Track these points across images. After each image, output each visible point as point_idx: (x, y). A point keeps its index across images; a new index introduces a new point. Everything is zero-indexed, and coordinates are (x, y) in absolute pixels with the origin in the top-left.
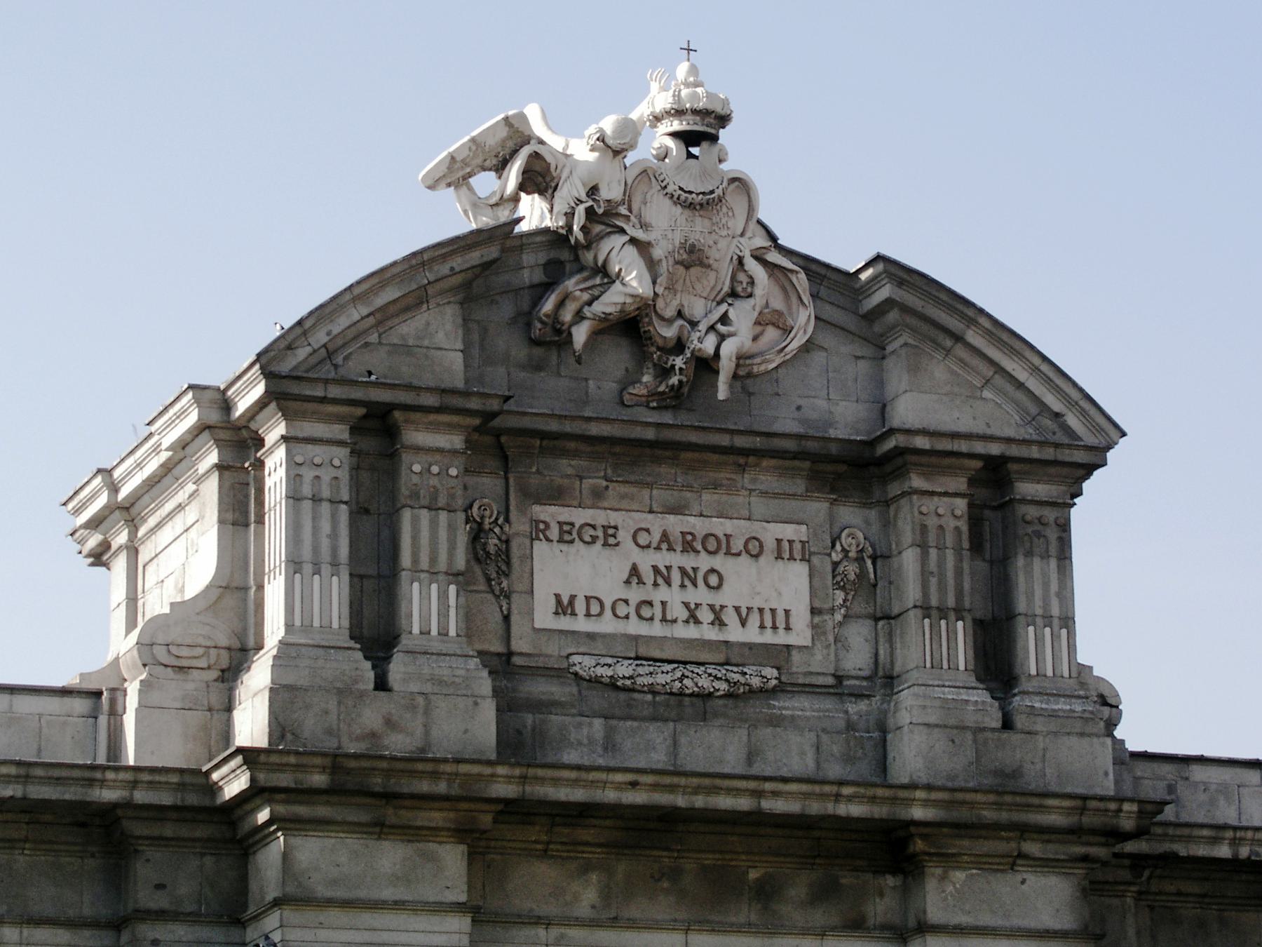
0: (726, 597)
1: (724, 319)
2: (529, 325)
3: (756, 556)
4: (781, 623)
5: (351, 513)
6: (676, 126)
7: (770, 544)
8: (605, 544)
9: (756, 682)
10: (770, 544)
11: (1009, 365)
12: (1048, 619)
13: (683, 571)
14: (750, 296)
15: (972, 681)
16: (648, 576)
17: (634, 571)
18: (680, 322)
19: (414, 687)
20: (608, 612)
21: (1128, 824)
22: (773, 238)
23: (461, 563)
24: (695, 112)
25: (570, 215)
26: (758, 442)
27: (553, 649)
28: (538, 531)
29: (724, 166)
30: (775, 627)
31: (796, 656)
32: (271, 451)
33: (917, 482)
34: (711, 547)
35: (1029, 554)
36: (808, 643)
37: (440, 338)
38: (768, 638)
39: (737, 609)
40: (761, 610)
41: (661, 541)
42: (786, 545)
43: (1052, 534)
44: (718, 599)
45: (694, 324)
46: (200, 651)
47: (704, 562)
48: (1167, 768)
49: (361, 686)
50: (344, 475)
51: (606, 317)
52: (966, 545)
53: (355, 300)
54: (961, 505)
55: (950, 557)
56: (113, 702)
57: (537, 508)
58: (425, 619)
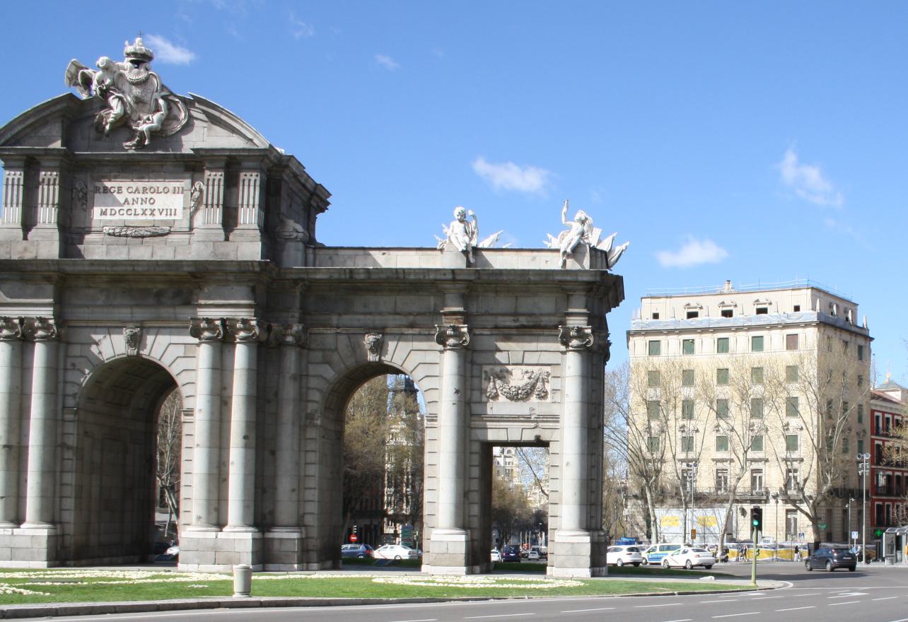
1: (148, 119)
3: (166, 193)
10: (171, 189)
15: (220, 226)
16: (131, 202)
19: (35, 239)
23: (56, 201)
30: (171, 215)
36: (181, 218)
38: (169, 218)
39: (159, 210)
40: (167, 210)
42: (177, 189)
47: (149, 196)
48: (331, 252)
51: (112, 123)
55: (216, 188)
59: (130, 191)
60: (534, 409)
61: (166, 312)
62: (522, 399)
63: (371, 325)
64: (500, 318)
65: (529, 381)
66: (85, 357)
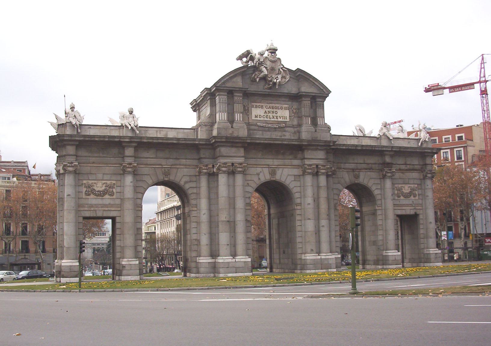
0: (279, 114)
1: (277, 77)
2: (251, 79)
4: (285, 118)
5: (227, 104)
6: (270, 51)
7: (284, 108)
8: (262, 108)
9: (282, 126)
10: (284, 108)
11: (316, 83)
12: (321, 117)
13: (272, 111)
14: (281, 74)
15: (311, 125)
16: (267, 112)
17: (266, 111)
18: (271, 78)
20: (262, 116)
21: (332, 144)
22: (284, 66)
24: (273, 49)
25: (256, 64)
26: (282, 94)
27: (255, 122)
28: (253, 106)
29: (276, 57)
31: (287, 122)
32: (217, 96)
33: (303, 99)
34: (276, 108)
35: (319, 108)
37: (239, 81)
38: (284, 120)
39: (279, 116)
41: (269, 107)
42: (286, 108)
43: (322, 106)
44: (277, 115)
45: (273, 78)
46: (208, 123)
47: (275, 110)
49: (229, 128)
50: (226, 99)
52: (310, 107)
53: (228, 76)
54: (309, 102)
55: (308, 108)
56: (197, 130)
57: (252, 103)
58: (238, 119)
59: (266, 107)
60: (413, 202)
61: (287, 162)
62: (409, 198)
63: (356, 168)
64: (401, 166)
65: (410, 190)
66: (252, 180)
